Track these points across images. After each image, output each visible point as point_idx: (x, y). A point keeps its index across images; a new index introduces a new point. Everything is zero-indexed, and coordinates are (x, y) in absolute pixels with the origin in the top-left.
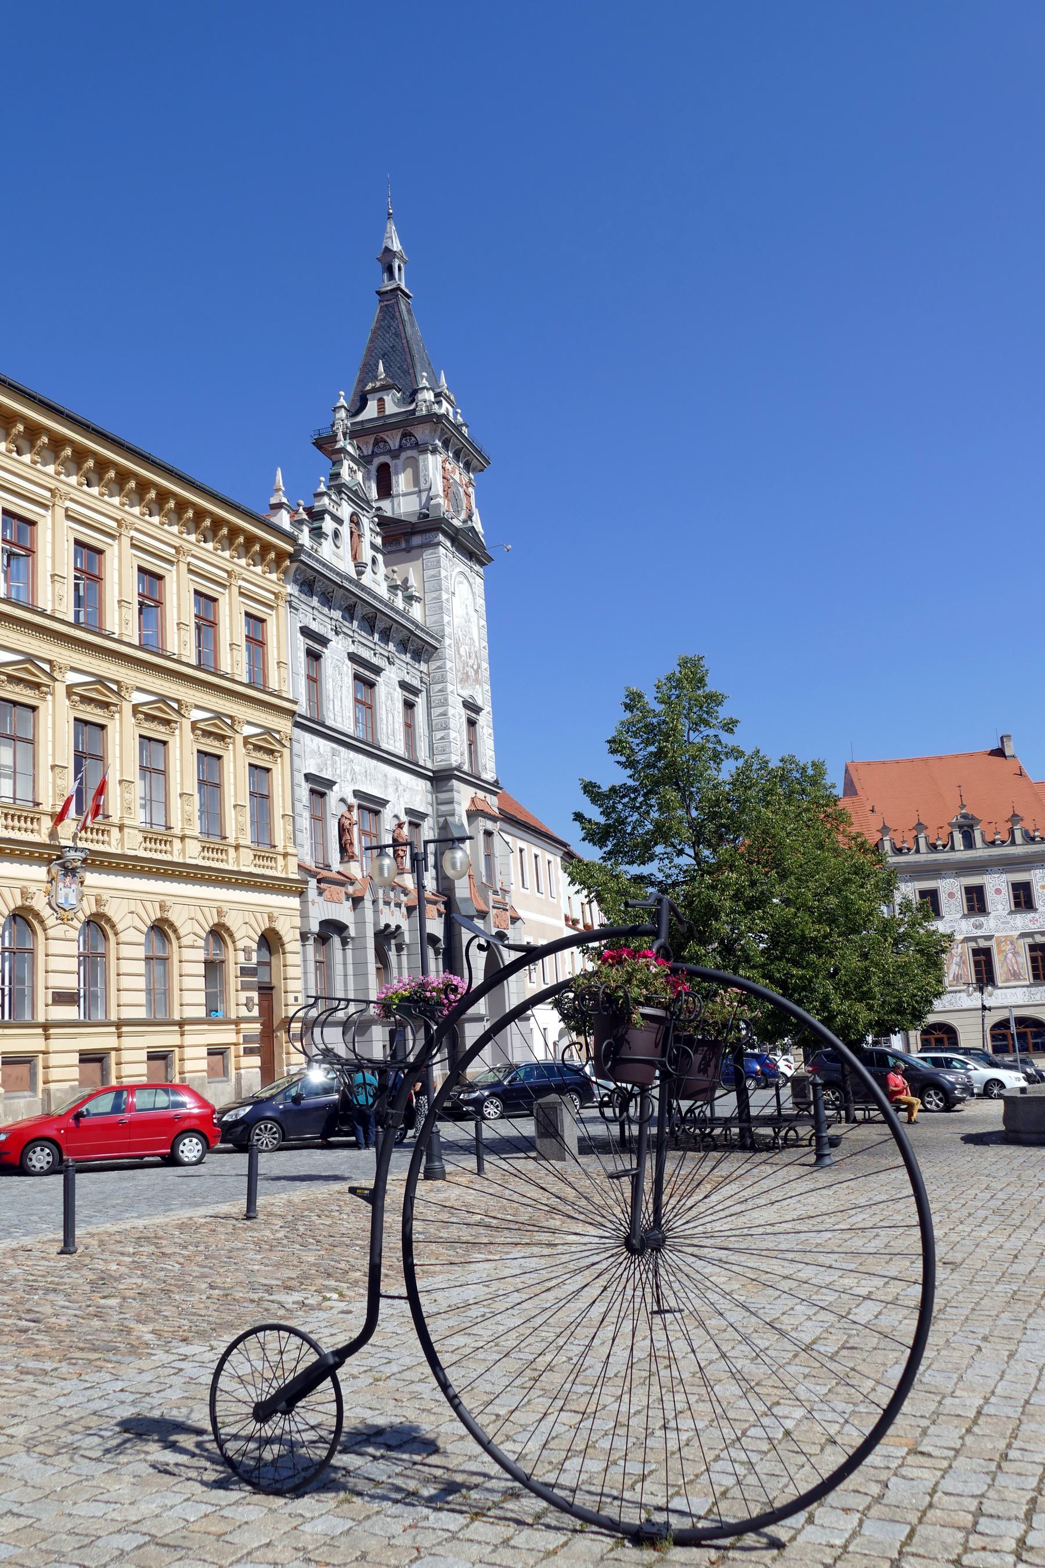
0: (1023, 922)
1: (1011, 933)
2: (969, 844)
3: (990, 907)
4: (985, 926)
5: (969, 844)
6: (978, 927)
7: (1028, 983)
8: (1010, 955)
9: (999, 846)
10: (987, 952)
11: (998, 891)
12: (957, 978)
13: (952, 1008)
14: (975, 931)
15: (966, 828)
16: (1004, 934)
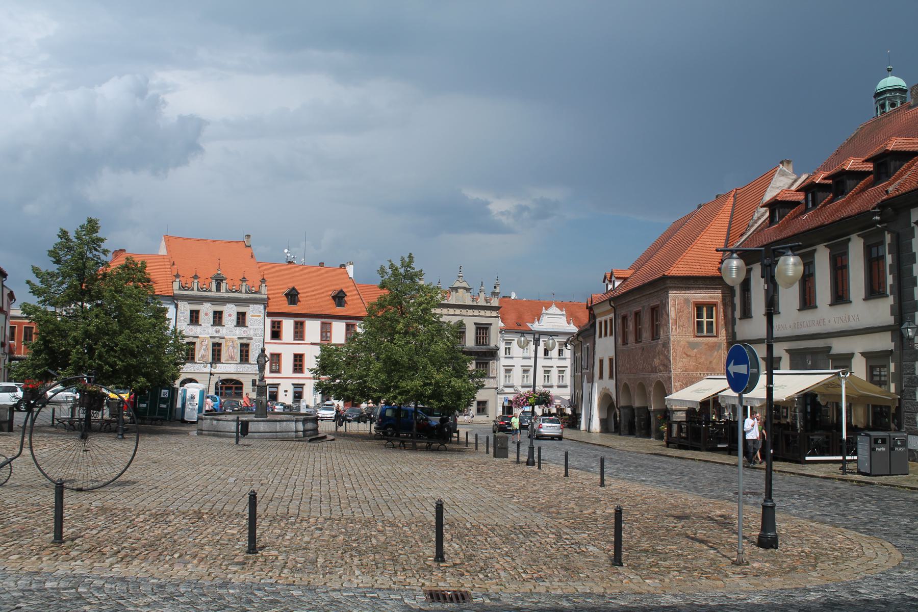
0: (240, 331)
1: (233, 337)
2: (218, 289)
3: (224, 322)
4: (221, 332)
5: (218, 289)
6: (217, 332)
7: (238, 362)
8: (231, 348)
9: (233, 292)
10: (220, 344)
11: (230, 315)
12: (203, 356)
13: (198, 372)
14: (215, 334)
15: (219, 281)
16: (230, 337)
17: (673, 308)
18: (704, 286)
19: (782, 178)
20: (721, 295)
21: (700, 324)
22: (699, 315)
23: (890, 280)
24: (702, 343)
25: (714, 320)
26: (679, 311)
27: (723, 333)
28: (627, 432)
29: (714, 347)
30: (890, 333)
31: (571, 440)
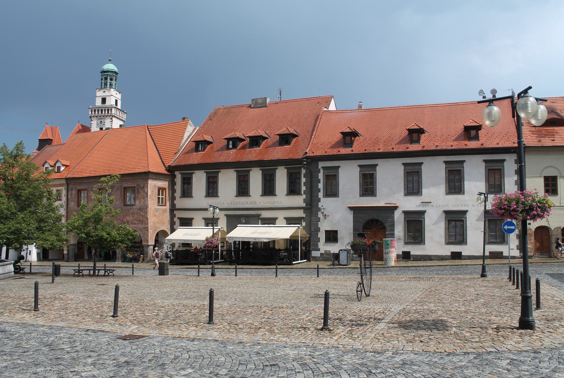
17: (150, 190)
18: (162, 179)
19: (190, 127)
20: (167, 184)
21: (159, 198)
22: (159, 195)
23: (303, 188)
24: (160, 209)
25: (164, 197)
26: (152, 192)
27: (168, 204)
28: (73, 260)
29: (164, 211)
30: (302, 210)
31: (40, 266)
